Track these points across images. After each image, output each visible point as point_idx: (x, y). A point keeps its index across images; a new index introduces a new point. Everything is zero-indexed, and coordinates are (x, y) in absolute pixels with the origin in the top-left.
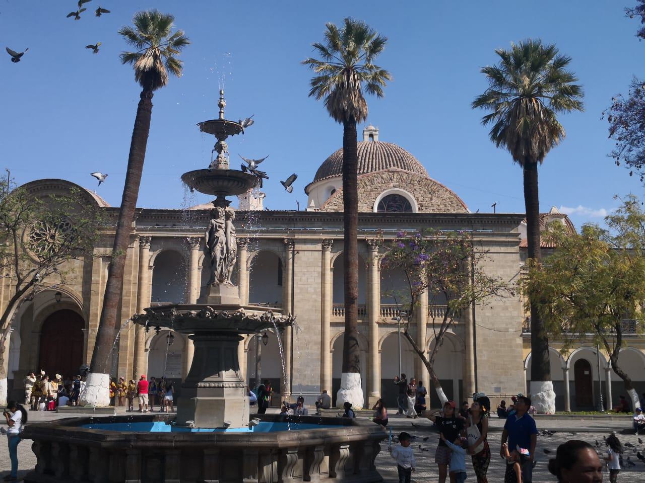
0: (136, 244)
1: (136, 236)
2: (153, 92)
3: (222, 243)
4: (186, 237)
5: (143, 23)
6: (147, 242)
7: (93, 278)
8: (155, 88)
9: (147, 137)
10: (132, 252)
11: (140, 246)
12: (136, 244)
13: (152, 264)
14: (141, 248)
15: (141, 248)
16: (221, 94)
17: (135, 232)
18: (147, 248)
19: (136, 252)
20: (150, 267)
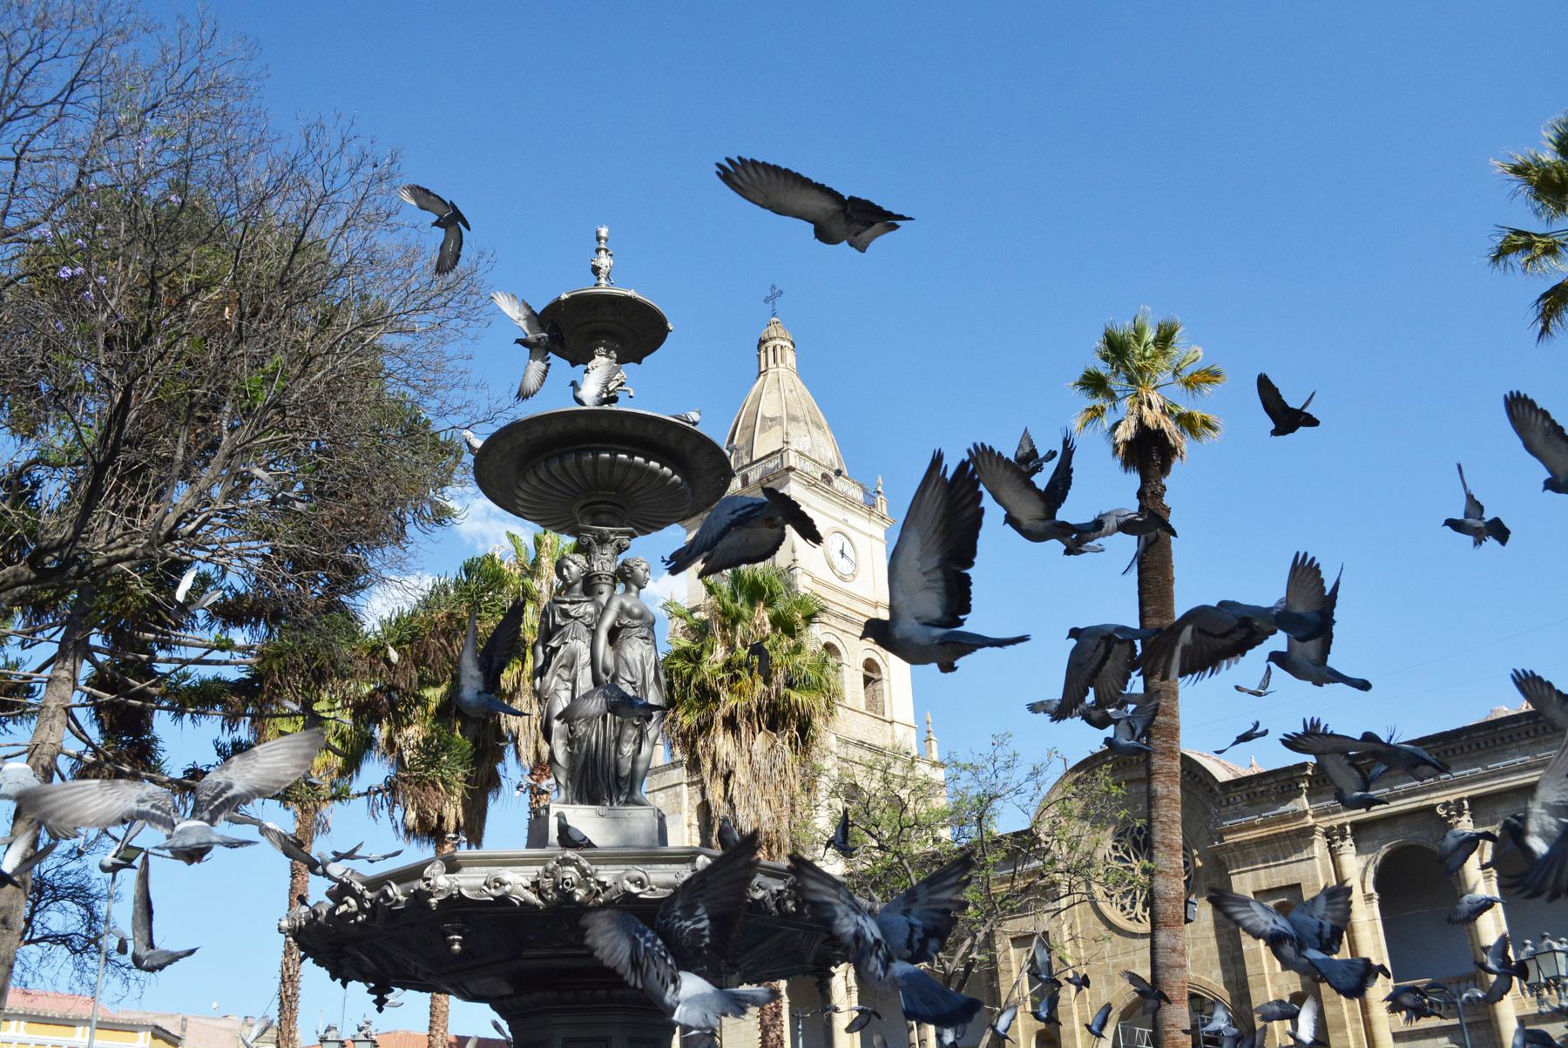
0: (1319, 846)
1: (1311, 830)
2: (1164, 481)
3: (570, 665)
4: (1433, 807)
5: (1116, 349)
6: (1343, 838)
7: (1244, 947)
8: (1165, 469)
9: (1170, 581)
10: (1314, 869)
11: (1332, 851)
12: (1319, 846)
13: (1370, 889)
14: (1334, 854)
15: (1334, 854)
16: (599, 239)
17: (1310, 821)
18: (1348, 849)
19: (1325, 867)
20: (1369, 898)
